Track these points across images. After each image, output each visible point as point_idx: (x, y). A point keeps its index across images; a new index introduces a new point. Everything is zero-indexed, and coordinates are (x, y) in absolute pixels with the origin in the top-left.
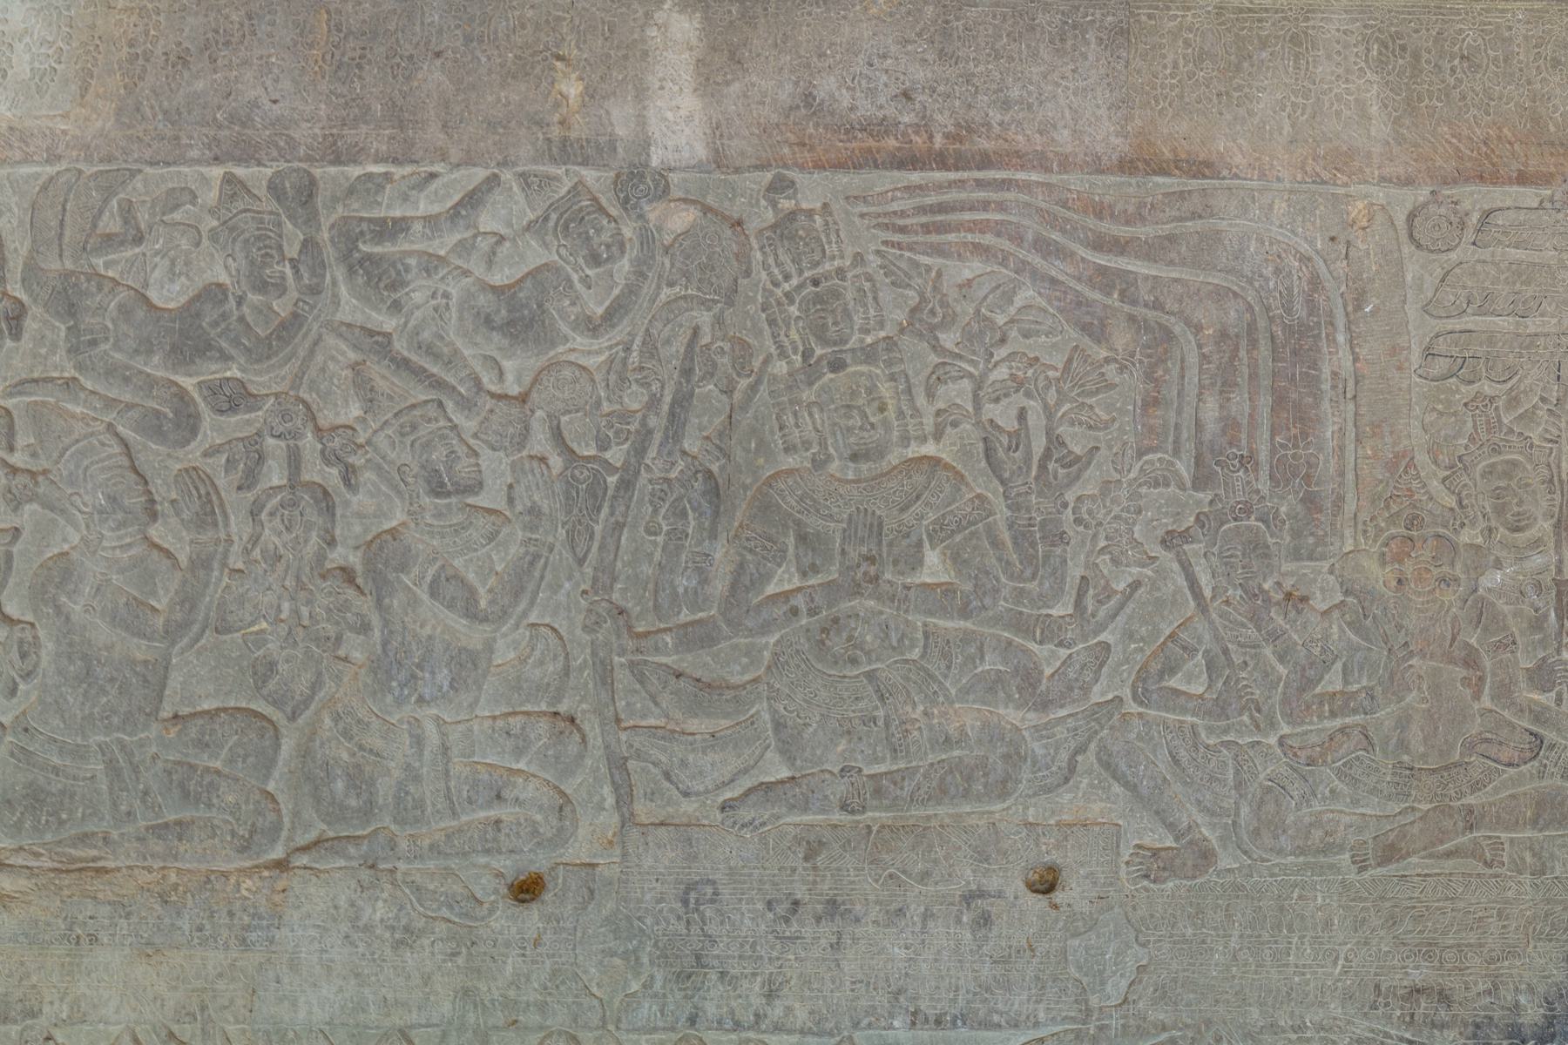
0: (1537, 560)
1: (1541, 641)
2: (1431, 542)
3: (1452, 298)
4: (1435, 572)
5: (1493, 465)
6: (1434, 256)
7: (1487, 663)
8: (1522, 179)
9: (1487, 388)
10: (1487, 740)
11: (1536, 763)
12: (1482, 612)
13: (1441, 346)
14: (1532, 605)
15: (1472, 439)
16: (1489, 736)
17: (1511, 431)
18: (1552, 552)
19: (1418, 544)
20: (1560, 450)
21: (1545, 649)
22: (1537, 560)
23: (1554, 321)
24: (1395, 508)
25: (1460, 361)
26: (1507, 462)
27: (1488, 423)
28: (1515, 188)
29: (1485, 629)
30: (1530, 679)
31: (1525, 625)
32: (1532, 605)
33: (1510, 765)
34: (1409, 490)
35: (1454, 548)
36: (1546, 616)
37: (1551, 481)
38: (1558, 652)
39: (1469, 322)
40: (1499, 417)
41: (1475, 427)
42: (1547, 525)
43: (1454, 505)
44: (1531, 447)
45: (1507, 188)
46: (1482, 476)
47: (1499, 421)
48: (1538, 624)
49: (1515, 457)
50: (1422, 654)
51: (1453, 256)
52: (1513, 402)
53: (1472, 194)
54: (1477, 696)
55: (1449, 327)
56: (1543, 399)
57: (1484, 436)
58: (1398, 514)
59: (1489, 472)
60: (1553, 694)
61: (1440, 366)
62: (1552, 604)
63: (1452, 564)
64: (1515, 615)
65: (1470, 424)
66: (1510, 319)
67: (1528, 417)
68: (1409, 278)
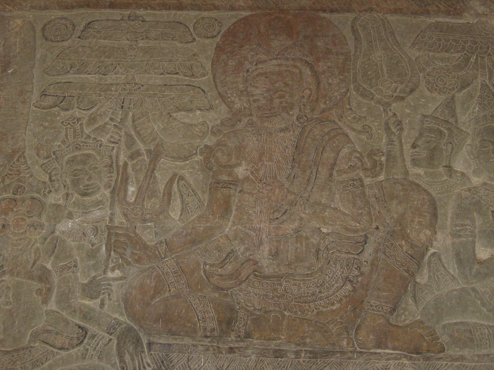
0: (97, 213)
1: (94, 265)
2: (29, 202)
3: (62, 65)
4: (28, 221)
5: (75, 157)
6: (54, 44)
7: (55, 279)
8: (112, 6)
9: (77, 113)
10: (48, 331)
11: (81, 348)
12: (56, 246)
13: (51, 91)
14: (90, 241)
15: (64, 142)
16: (50, 328)
17: (89, 137)
18: (108, 209)
19: (19, 203)
20: (119, 148)
21: (96, 270)
22: (97, 213)
23: (123, 77)
24: (7, 181)
25: (61, 98)
26: (84, 155)
27: (75, 132)
28: (108, 11)
29: (57, 257)
30: (84, 290)
31: (84, 255)
32: (90, 241)
33: (61, 349)
34: (18, 171)
35: (43, 205)
36: (99, 249)
37: (111, 166)
38: (105, 272)
39: (70, 77)
40: (82, 129)
41: (66, 136)
42: (107, 193)
43: (47, 180)
44: (101, 146)
45: (103, 11)
46: (67, 163)
47: (82, 131)
48: (93, 254)
49: (90, 152)
50: (11, 273)
51: (66, 44)
52: (92, 120)
53: (83, 14)
54: (45, 301)
55: (59, 81)
56: (111, 119)
57: (71, 139)
58: (9, 185)
59: (73, 160)
60: (98, 301)
61: (49, 101)
62: (104, 241)
63: (40, 215)
64: (78, 249)
65: (64, 133)
66: (97, 76)
67: (102, 129)
68: (38, 56)
